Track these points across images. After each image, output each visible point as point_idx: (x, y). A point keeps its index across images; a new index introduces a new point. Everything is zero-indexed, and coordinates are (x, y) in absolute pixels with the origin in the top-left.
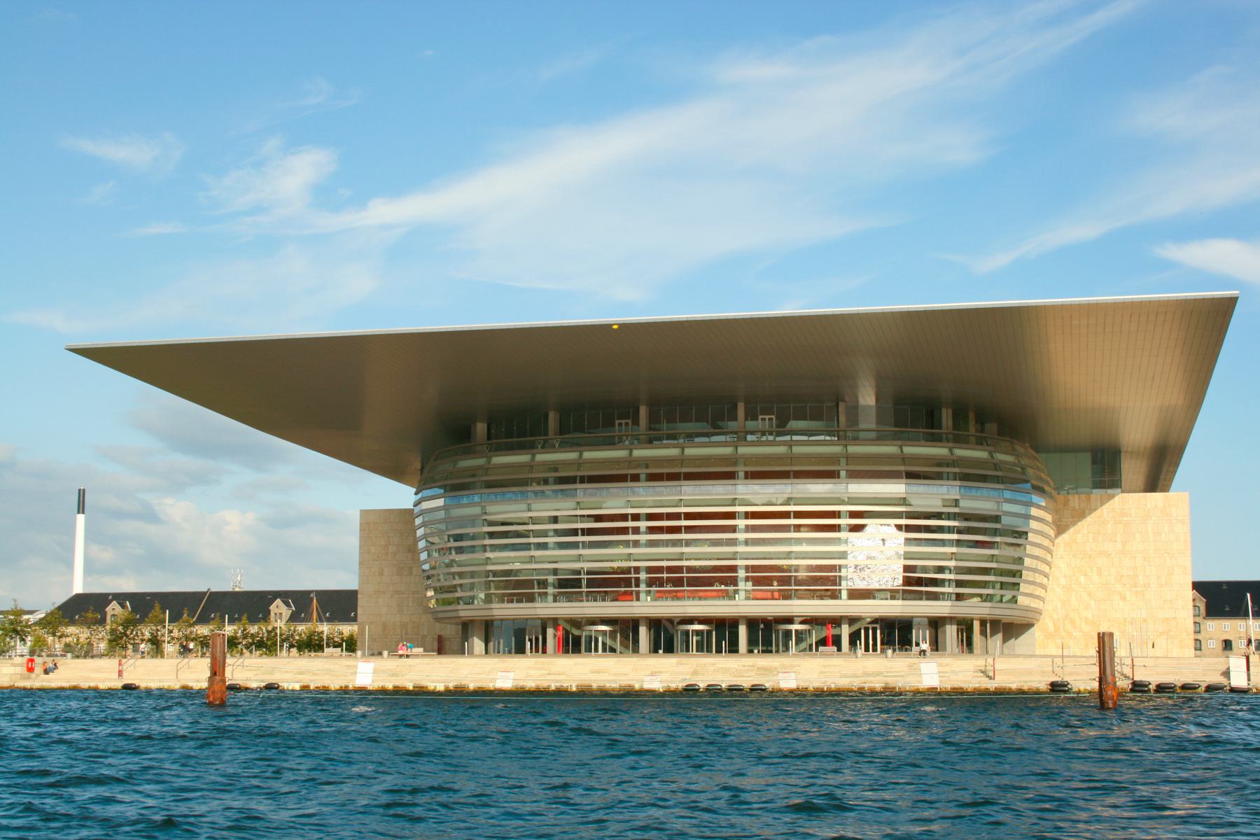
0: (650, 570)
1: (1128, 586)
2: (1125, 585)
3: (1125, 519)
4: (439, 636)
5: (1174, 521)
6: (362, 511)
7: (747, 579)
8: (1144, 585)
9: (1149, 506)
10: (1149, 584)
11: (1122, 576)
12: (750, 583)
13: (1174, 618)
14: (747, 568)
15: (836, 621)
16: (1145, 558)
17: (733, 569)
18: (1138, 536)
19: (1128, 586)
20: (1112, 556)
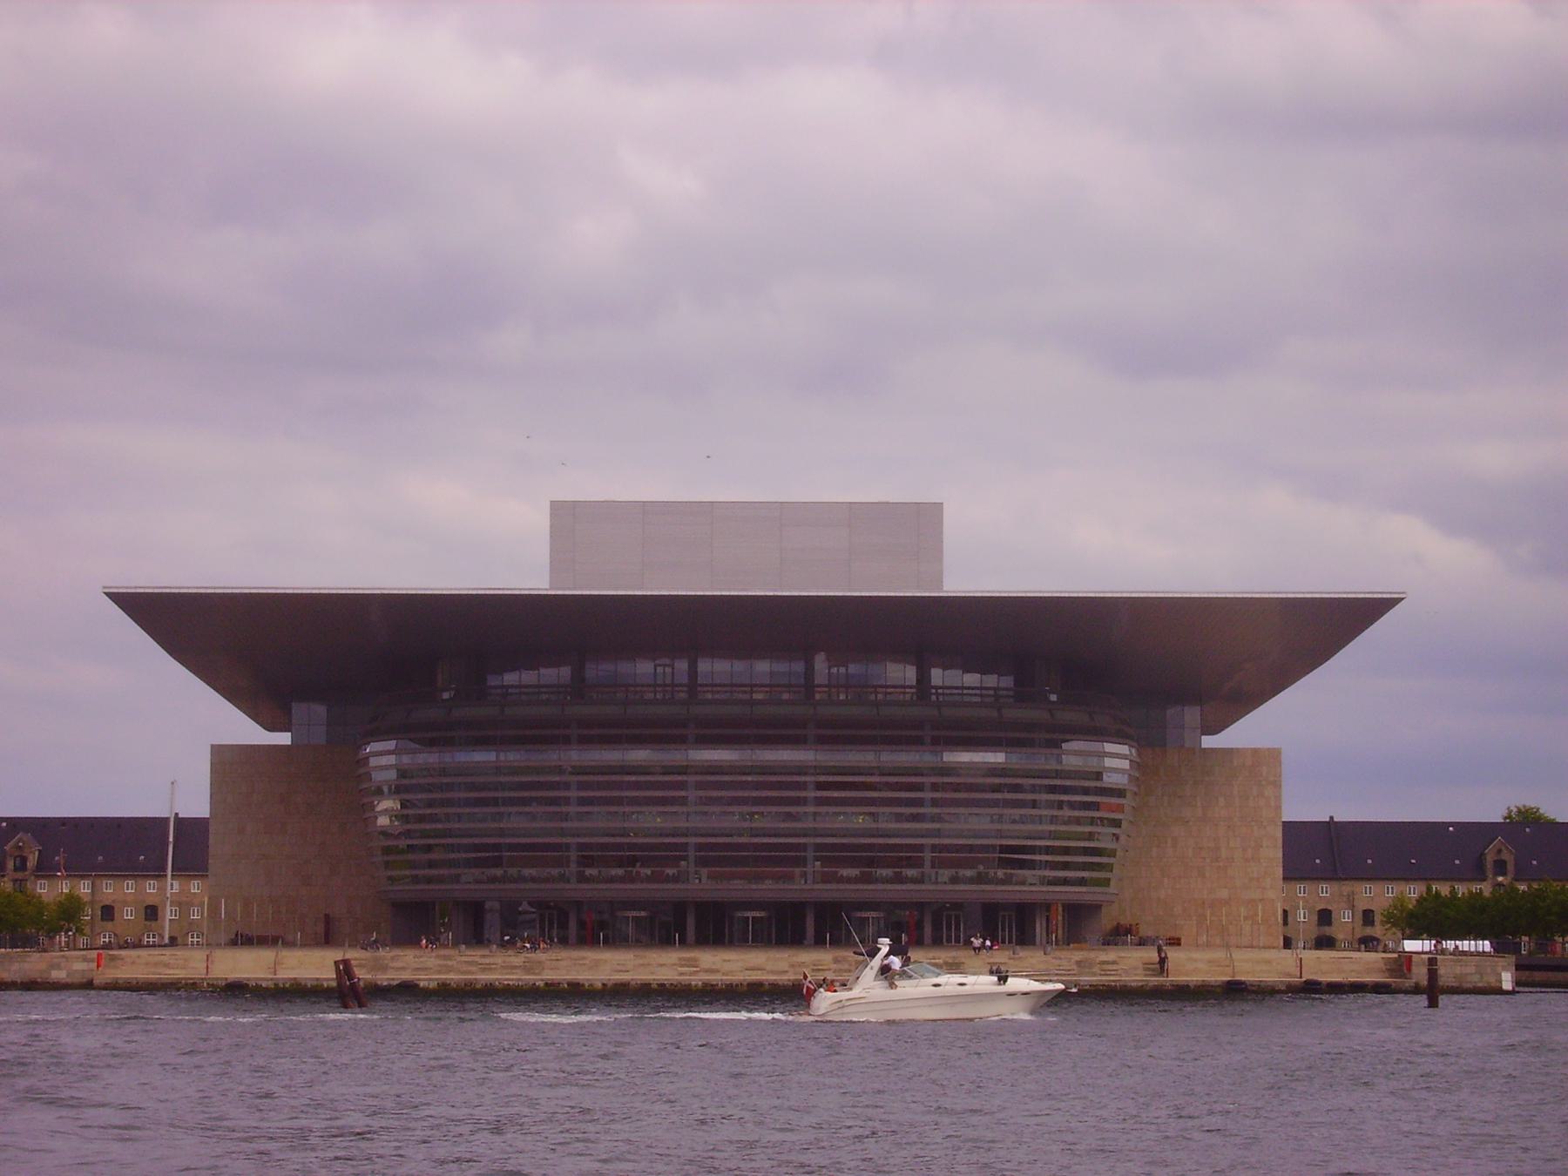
0: (700, 847)
1: (1208, 860)
2: (1204, 858)
3: (1207, 779)
4: (326, 915)
5: (1264, 783)
6: (212, 746)
7: (816, 858)
8: (1227, 858)
9: (1235, 764)
10: (1233, 858)
11: (1201, 848)
12: (818, 863)
13: (1261, 900)
14: (819, 847)
15: (920, 906)
16: (1229, 827)
17: (803, 847)
18: (1222, 800)
19: (1208, 860)
20: (1191, 823)
